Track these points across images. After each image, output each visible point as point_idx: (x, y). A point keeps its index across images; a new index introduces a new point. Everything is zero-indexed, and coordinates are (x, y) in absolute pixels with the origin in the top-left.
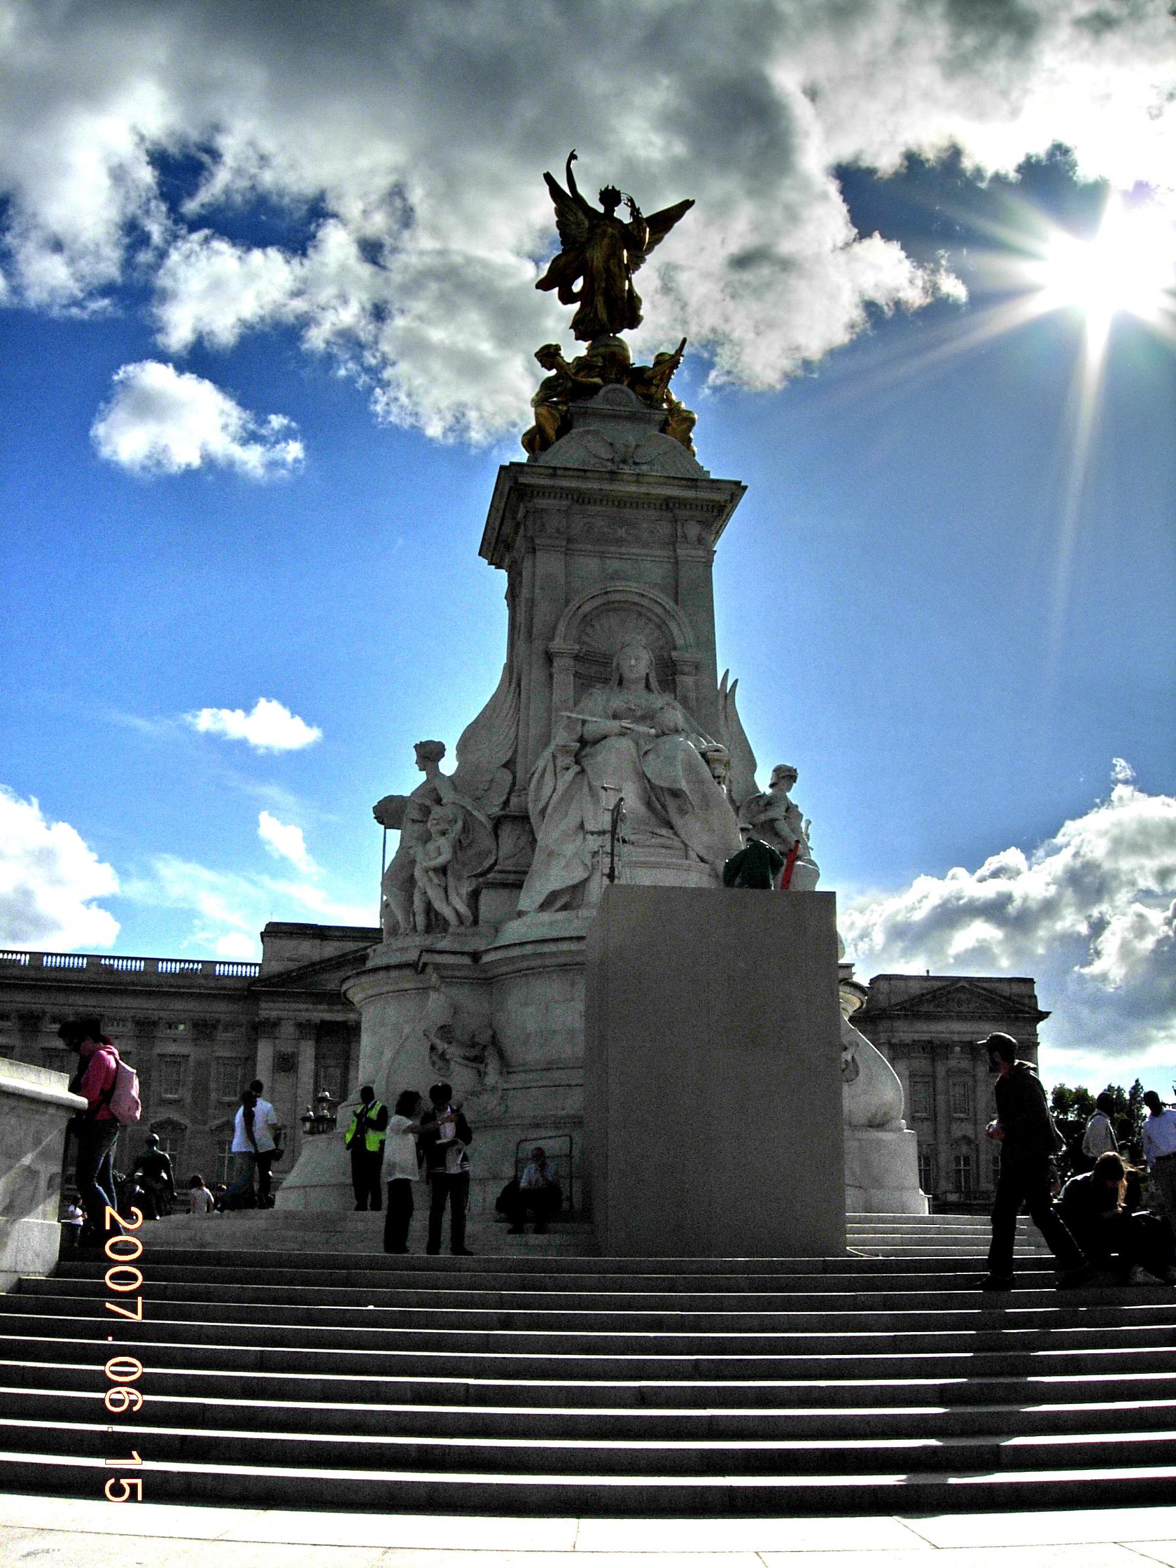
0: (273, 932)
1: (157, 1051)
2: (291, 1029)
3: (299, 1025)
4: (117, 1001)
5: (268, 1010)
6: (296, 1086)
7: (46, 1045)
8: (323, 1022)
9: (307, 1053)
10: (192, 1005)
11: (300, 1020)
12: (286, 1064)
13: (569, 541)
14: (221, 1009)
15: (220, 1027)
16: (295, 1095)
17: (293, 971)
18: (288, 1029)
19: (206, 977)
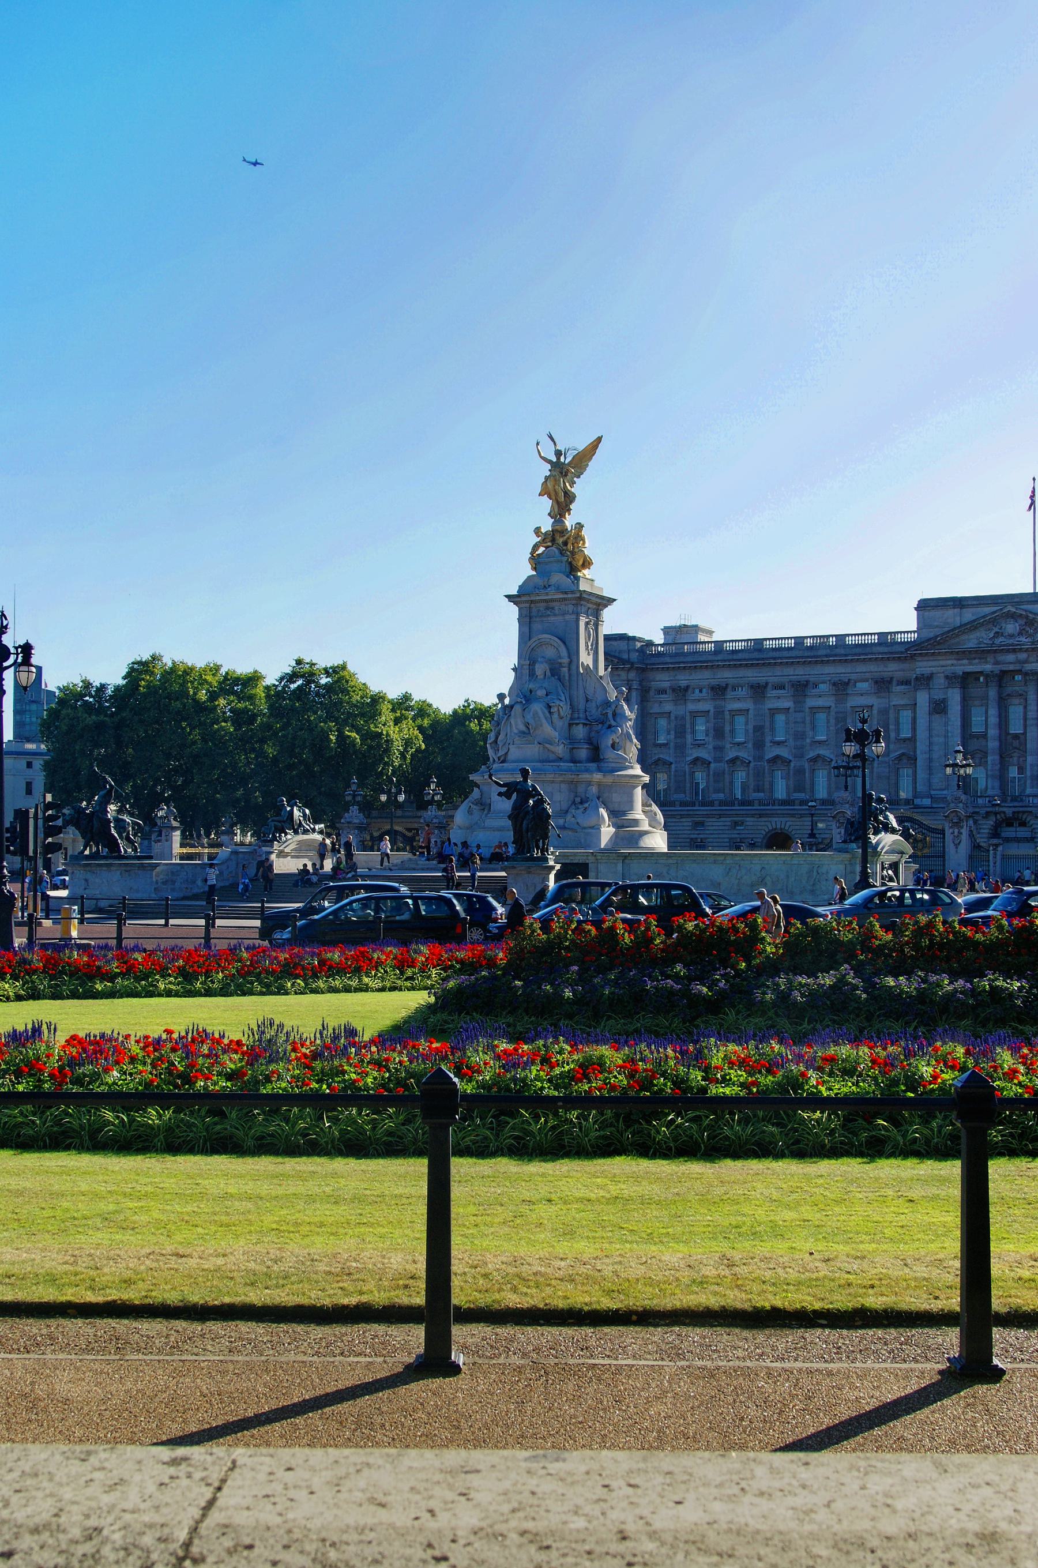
0: (924, 606)
1: (849, 705)
2: (942, 681)
3: (947, 677)
4: (818, 669)
5: (923, 667)
6: (946, 724)
7: (771, 706)
8: (966, 675)
9: (955, 697)
10: (872, 667)
11: (947, 673)
12: (939, 708)
13: (530, 618)
14: (893, 669)
15: (894, 683)
16: (947, 731)
17: (937, 636)
18: (940, 681)
19: (879, 644)
